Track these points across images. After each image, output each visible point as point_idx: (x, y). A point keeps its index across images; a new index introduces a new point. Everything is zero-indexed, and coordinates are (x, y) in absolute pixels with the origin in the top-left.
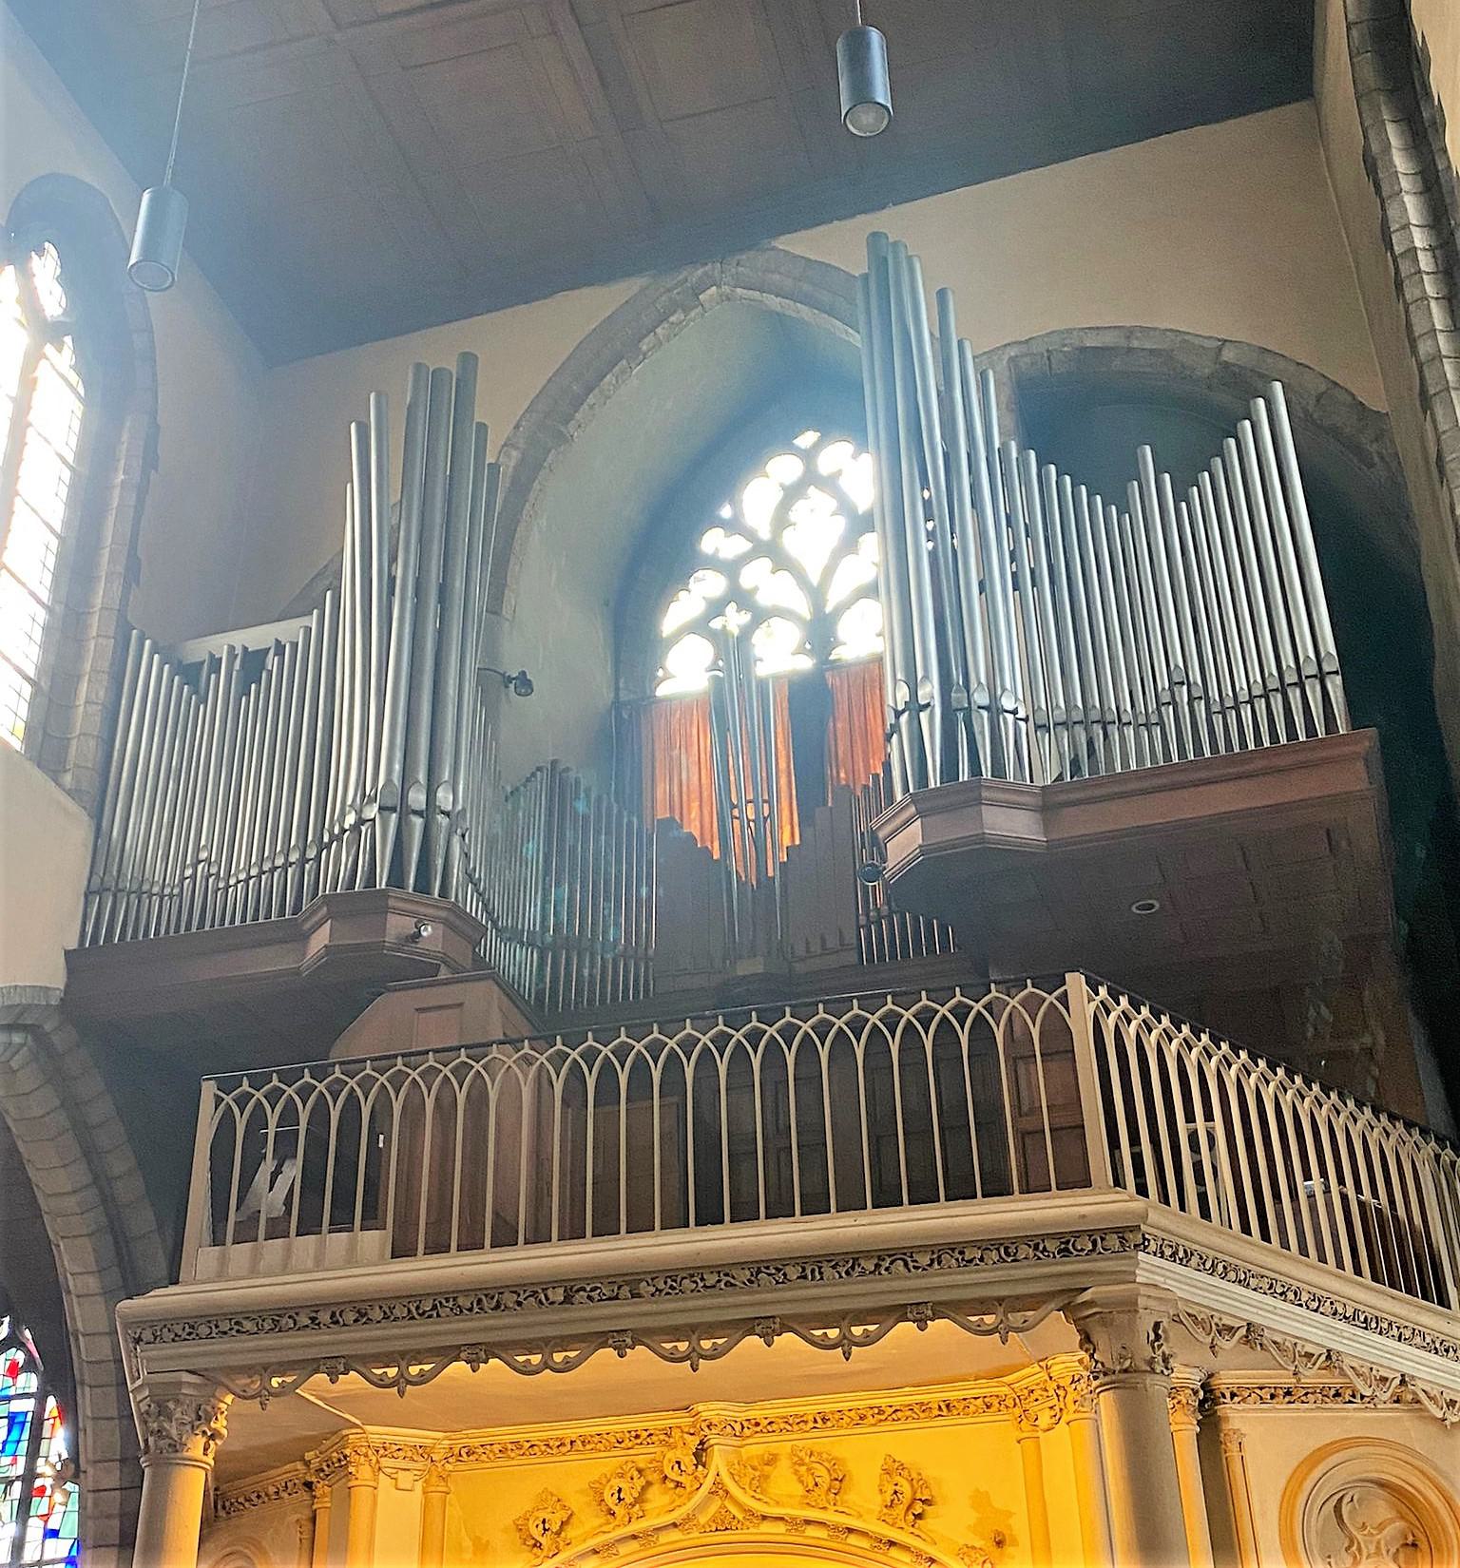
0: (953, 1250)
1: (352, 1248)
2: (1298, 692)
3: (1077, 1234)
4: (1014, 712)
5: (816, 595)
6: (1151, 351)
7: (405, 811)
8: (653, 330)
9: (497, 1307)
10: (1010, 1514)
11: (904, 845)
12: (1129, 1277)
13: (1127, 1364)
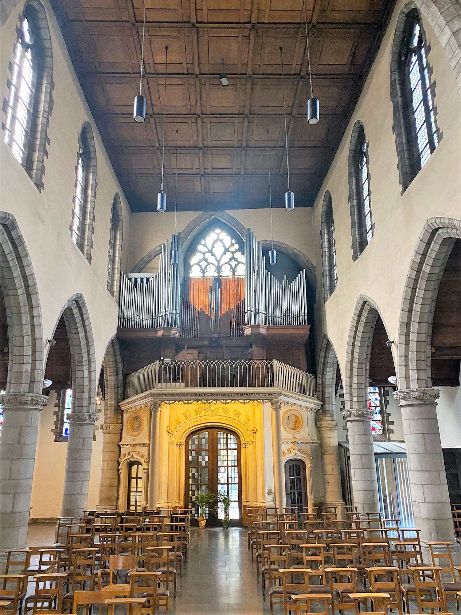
1: (180, 385)
5: (219, 262)
10: (250, 417)
11: (248, 331)
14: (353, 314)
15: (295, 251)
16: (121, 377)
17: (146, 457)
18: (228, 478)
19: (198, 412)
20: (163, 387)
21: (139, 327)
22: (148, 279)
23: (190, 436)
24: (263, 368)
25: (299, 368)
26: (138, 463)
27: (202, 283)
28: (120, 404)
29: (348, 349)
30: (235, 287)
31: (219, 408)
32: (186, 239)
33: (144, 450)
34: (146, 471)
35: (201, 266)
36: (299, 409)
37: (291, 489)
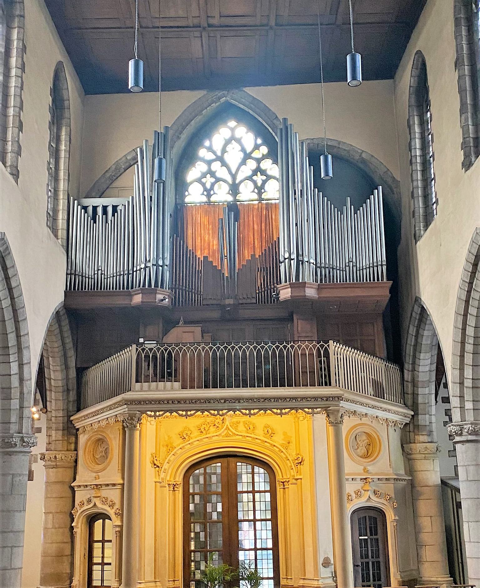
1: (172, 386)
4: (313, 263)
5: (234, 177)
8: (206, 108)
11: (285, 294)
12: (338, 406)
14: (463, 262)
16: (73, 373)
17: (117, 506)
18: (255, 539)
19: (202, 430)
20: (144, 389)
21: (101, 289)
22: (115, 208)
23: (191, 471)
24: (311, 355)
25: (373, 354)
26: (104, 517)
27: (207, 213)
28: (72, 418)
29: (456, 321)
30: (263, 219)
32: (179, 138)
33: (114, 495)
34: (118, 529)
35: (204, 185)
36: (374, 424)
37: (362, 557)
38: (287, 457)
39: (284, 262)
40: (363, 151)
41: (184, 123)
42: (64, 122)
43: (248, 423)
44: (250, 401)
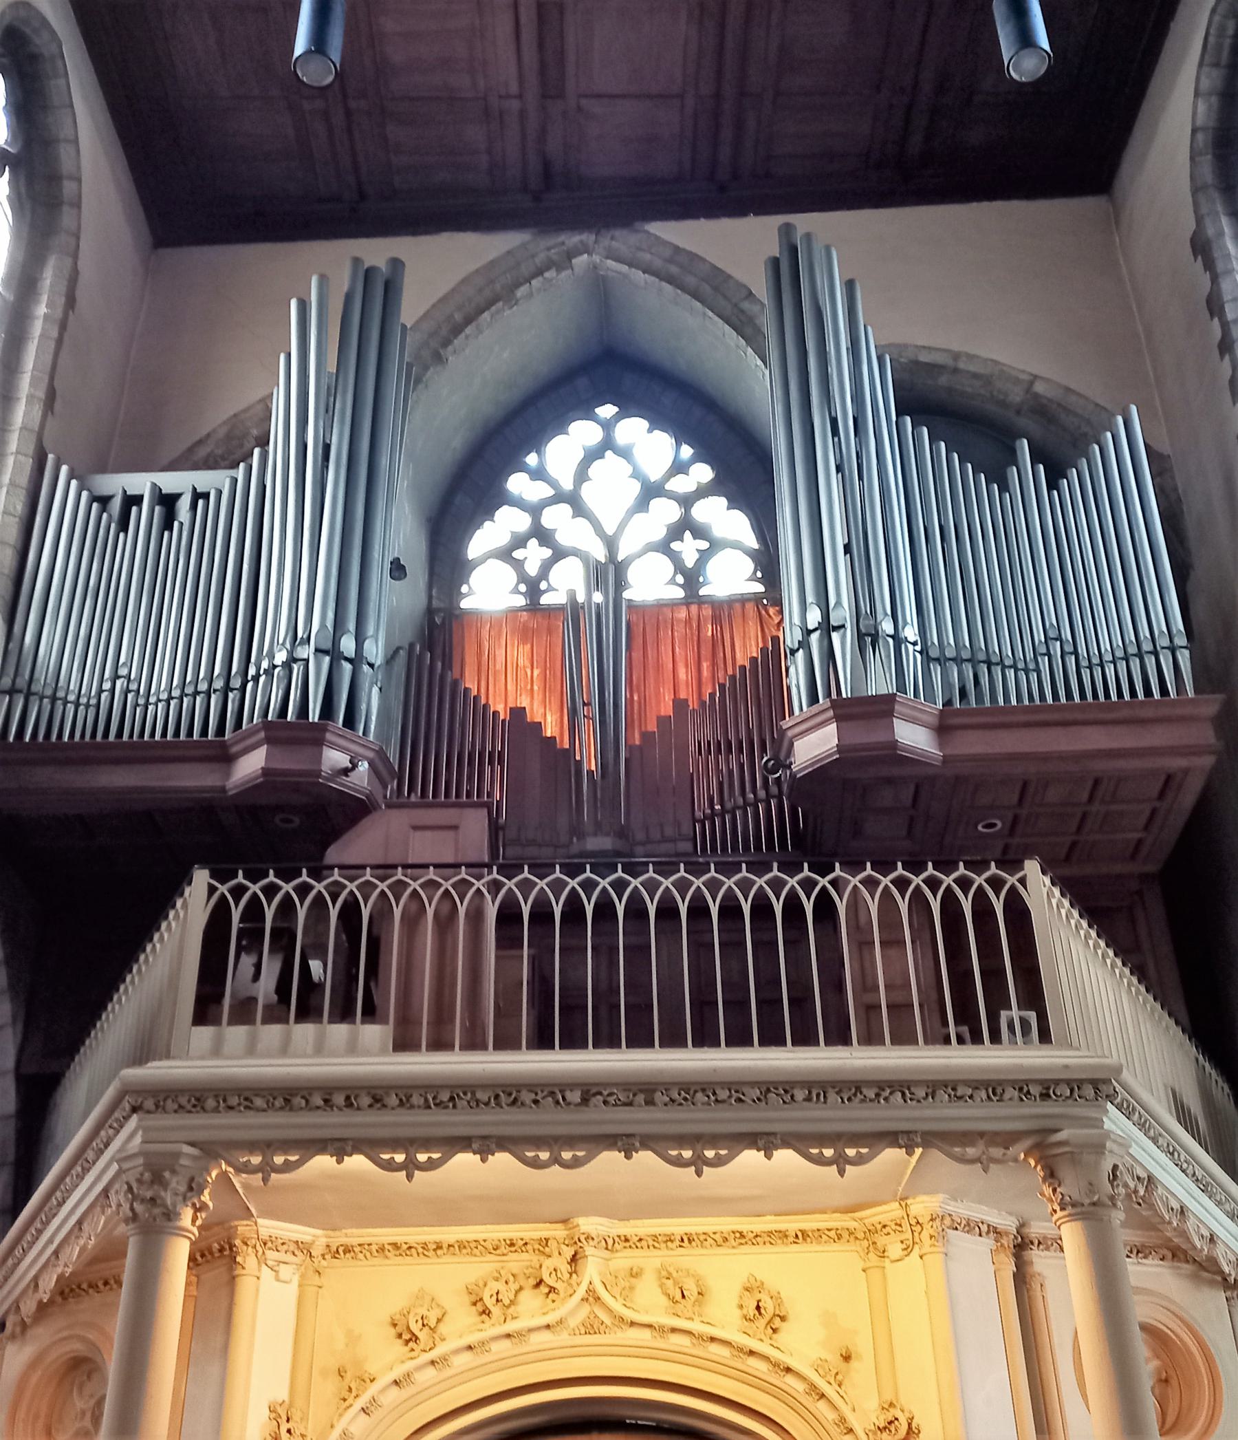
0: (946, 1087)
2: (1153, 658)
3: (1057, 1082)
4: (915, 644)
5: (611, 544)
6: (976, 376)
7: (335, 654)
9: (514, 1102)
13: (1096, 1198)
15: (1039, 388)
19: (490, 1302)
30: (706, 651)
31: (635, 1274)
38: (843, 1420)
39: (804, 644)
40: (1036, 377)
41: (456, 316)
42: (62, 239)
43: (675, 1274)
44: (699, 1095)
